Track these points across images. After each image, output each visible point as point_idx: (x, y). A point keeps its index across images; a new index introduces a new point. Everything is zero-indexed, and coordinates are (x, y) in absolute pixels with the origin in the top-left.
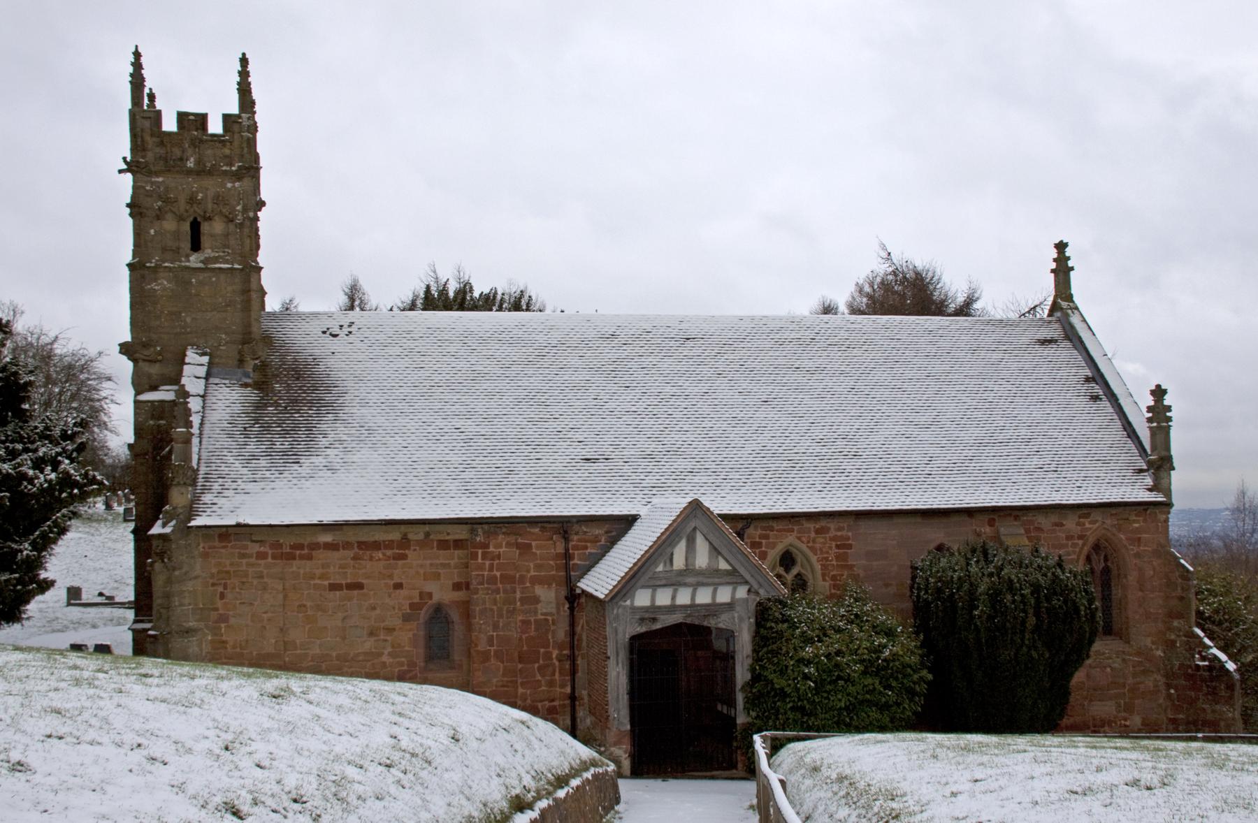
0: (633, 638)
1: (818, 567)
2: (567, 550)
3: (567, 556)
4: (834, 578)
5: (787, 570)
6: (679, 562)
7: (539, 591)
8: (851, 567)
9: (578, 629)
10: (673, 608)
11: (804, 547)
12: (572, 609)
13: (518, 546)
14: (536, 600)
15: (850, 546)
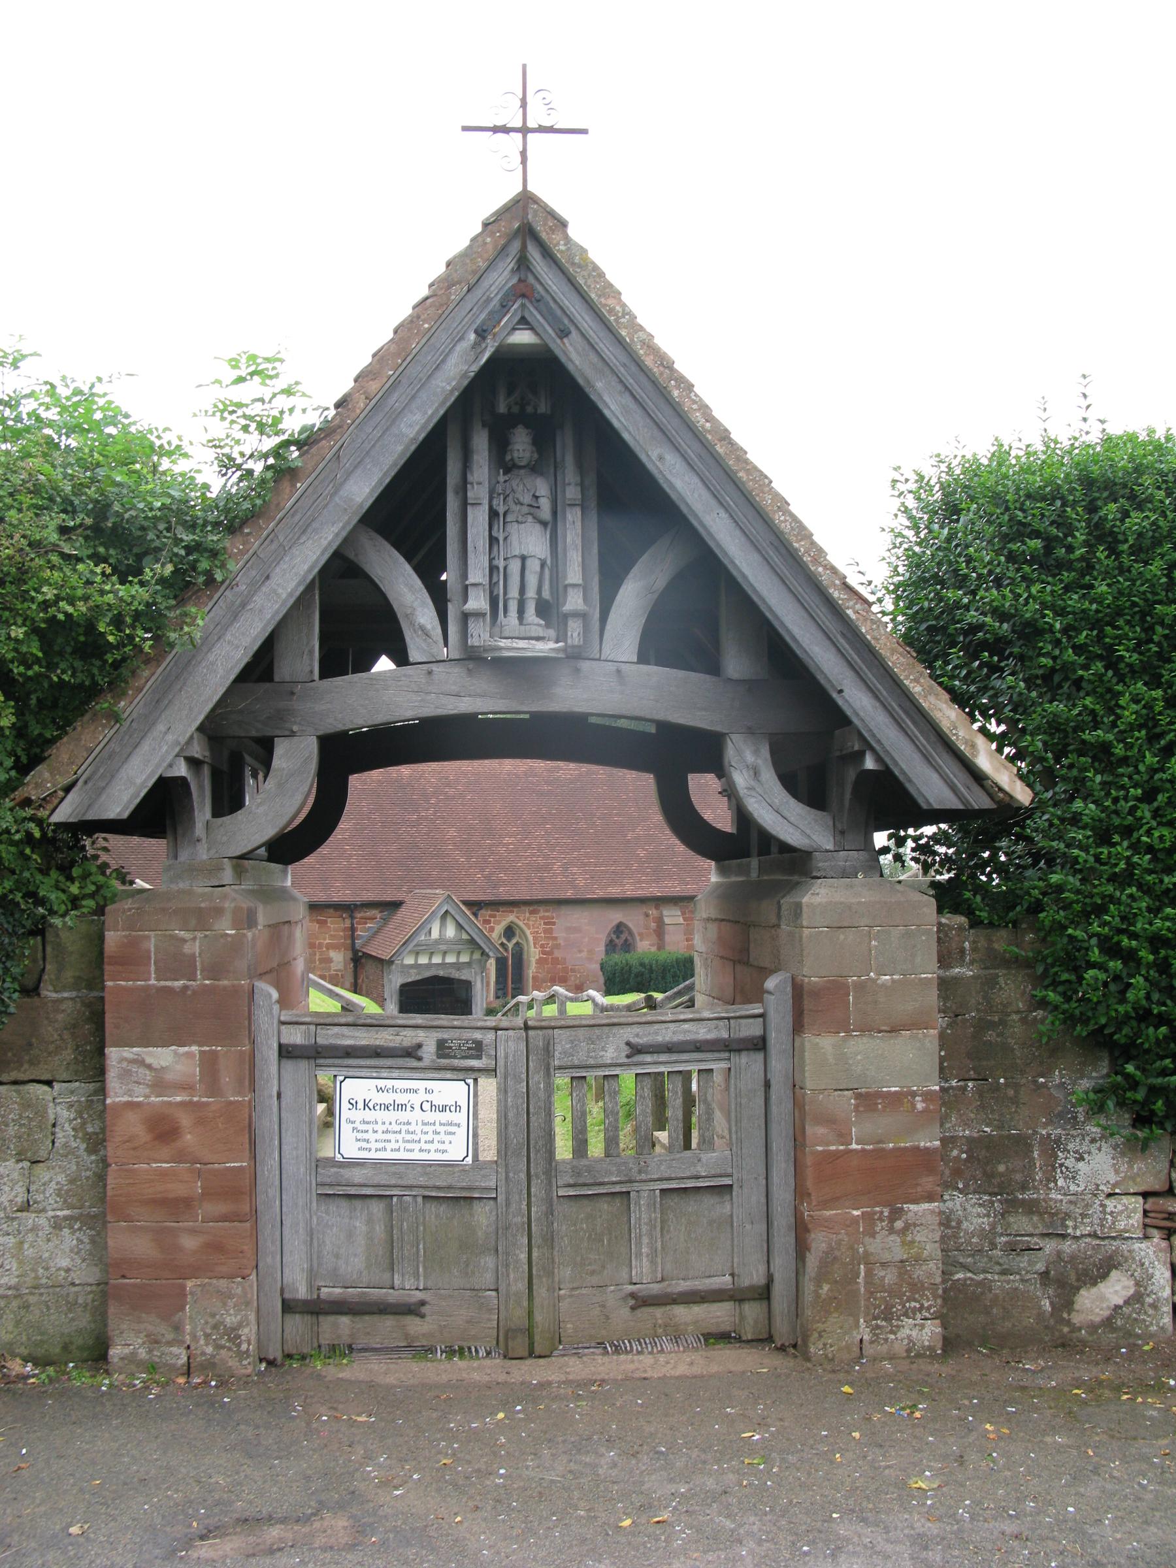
0: (403, 986)
1: (531, 938)
2: (352, 924)
3: (353, 929)
4: (542, 946)
5: (509, 940)
6: (435, 934)
7: (333, 954)
8: (555, 938)
9: (360, 981)
10: (429, 966)
11: (521, 924)
12: (356, 967)
13: (318, 922)
14: (330, 960)
15: (554, 924)
